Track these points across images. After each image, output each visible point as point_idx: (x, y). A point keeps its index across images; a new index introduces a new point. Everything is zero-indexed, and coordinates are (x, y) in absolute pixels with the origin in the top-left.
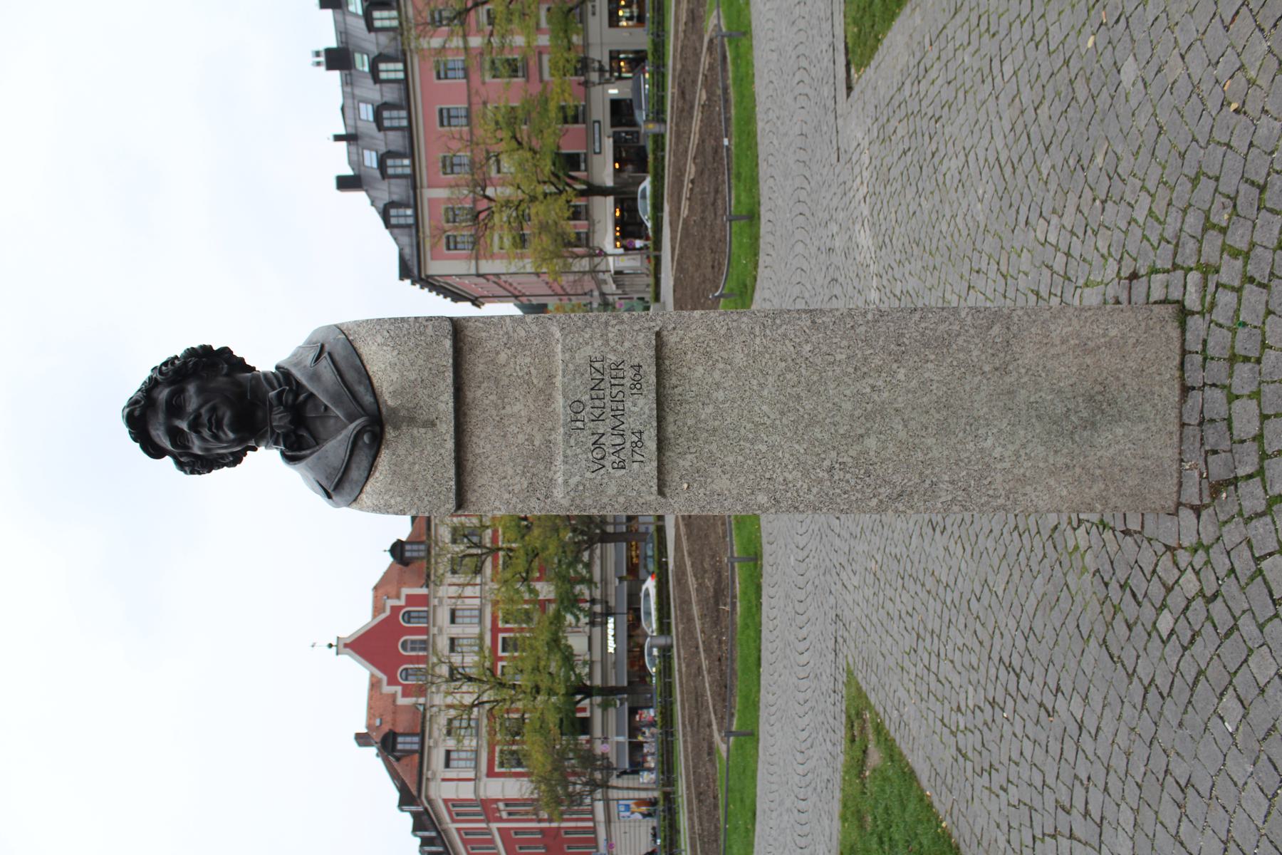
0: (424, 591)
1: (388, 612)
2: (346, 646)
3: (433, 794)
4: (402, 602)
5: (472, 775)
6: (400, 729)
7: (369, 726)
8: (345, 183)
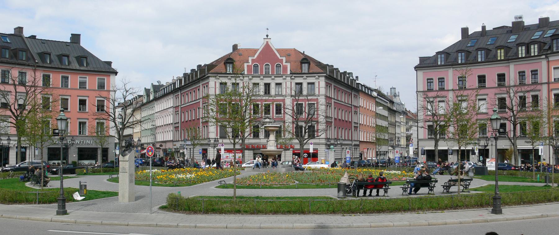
1: (280, 58)
2: (267, 42)
4: (284, 64)
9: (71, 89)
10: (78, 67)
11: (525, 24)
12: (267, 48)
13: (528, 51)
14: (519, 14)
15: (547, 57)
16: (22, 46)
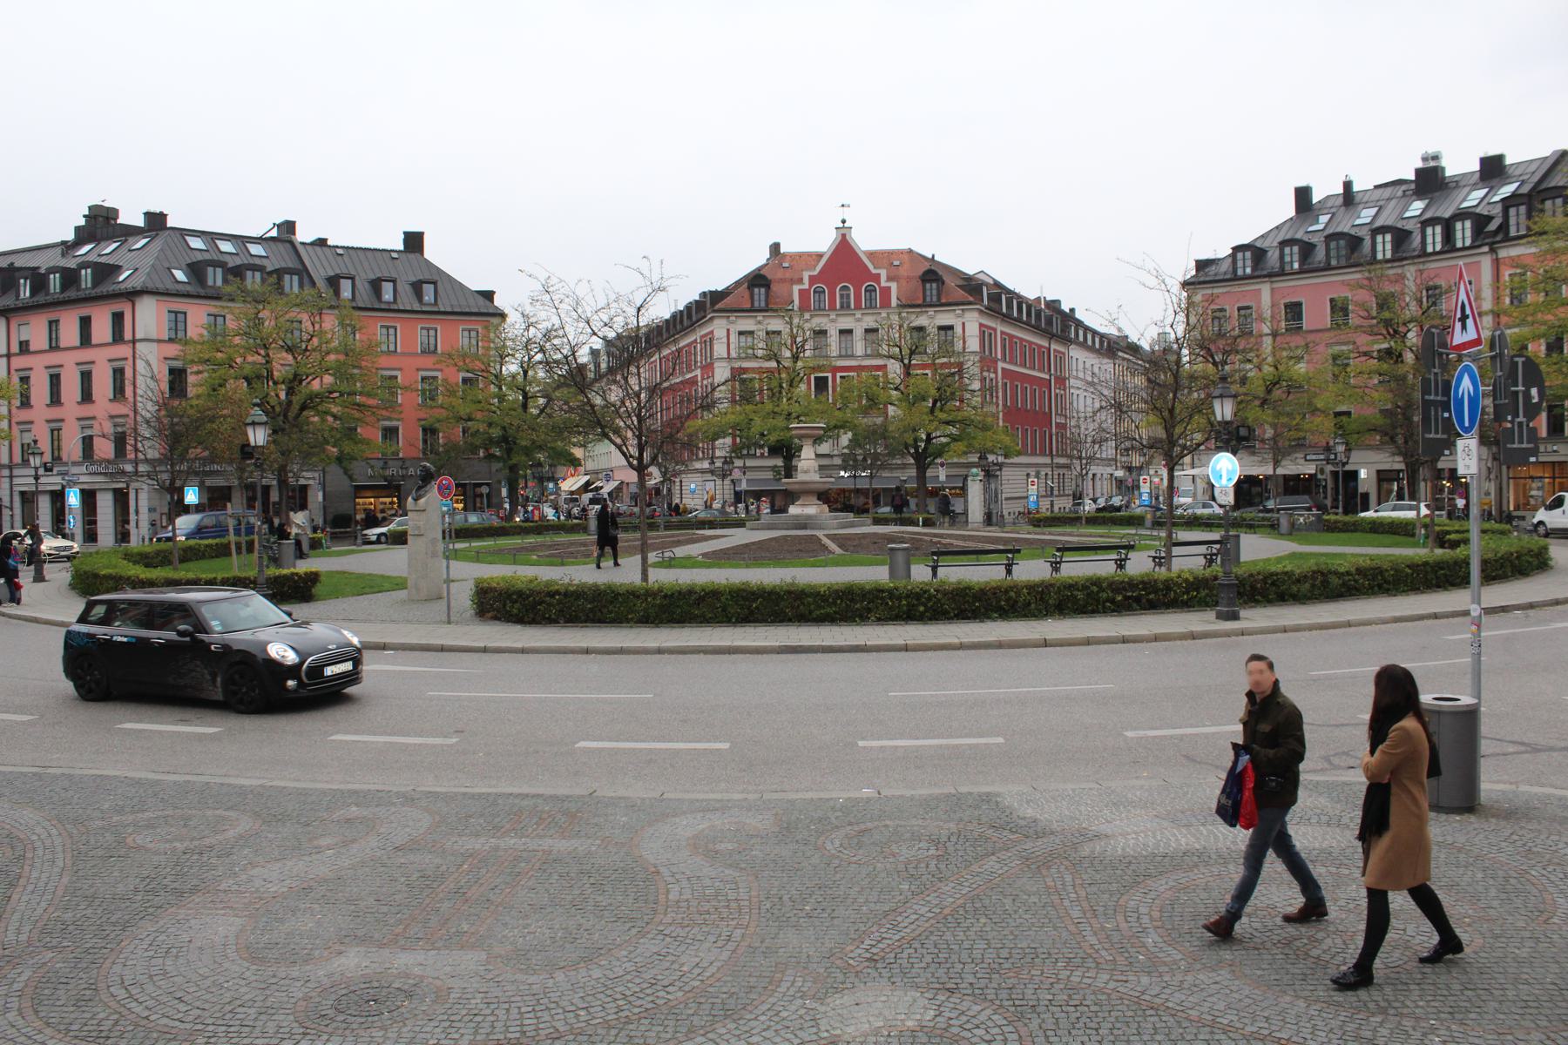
0: (894, 302)
1: (874, 271)
2: (844, 236)
3: (716, 322)
4: (884, 283)
5: (733, 354)
6: (774, 287)
7: (784, 255)
8: (1303, 195)
9: (403, 354)
10: (417, 307)
11: (1448, 174)
12: (844, 247)
13: (1448, 236)
14: (1431, 151)
15: (1493, 250)
16: (290, 263)
